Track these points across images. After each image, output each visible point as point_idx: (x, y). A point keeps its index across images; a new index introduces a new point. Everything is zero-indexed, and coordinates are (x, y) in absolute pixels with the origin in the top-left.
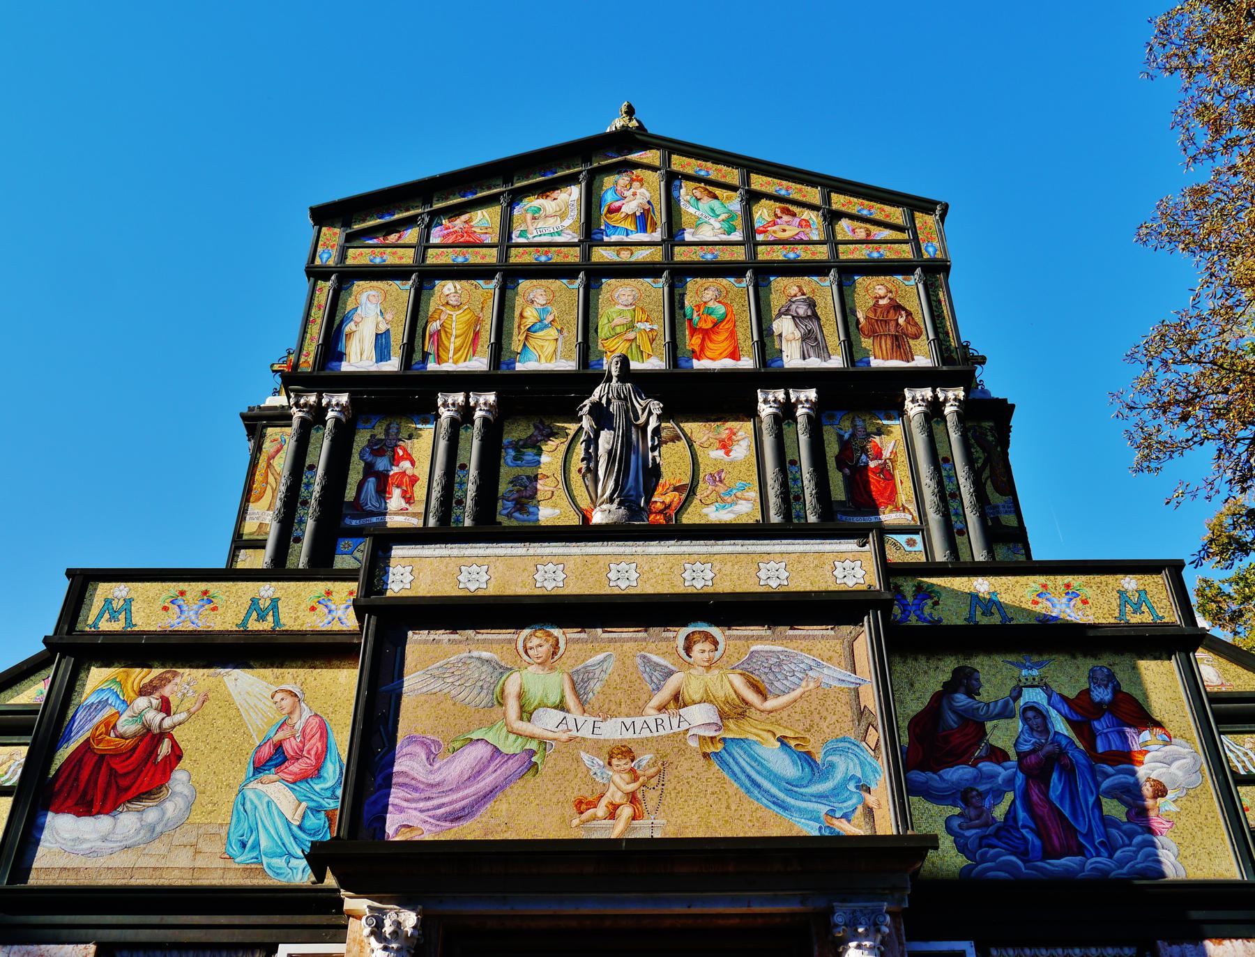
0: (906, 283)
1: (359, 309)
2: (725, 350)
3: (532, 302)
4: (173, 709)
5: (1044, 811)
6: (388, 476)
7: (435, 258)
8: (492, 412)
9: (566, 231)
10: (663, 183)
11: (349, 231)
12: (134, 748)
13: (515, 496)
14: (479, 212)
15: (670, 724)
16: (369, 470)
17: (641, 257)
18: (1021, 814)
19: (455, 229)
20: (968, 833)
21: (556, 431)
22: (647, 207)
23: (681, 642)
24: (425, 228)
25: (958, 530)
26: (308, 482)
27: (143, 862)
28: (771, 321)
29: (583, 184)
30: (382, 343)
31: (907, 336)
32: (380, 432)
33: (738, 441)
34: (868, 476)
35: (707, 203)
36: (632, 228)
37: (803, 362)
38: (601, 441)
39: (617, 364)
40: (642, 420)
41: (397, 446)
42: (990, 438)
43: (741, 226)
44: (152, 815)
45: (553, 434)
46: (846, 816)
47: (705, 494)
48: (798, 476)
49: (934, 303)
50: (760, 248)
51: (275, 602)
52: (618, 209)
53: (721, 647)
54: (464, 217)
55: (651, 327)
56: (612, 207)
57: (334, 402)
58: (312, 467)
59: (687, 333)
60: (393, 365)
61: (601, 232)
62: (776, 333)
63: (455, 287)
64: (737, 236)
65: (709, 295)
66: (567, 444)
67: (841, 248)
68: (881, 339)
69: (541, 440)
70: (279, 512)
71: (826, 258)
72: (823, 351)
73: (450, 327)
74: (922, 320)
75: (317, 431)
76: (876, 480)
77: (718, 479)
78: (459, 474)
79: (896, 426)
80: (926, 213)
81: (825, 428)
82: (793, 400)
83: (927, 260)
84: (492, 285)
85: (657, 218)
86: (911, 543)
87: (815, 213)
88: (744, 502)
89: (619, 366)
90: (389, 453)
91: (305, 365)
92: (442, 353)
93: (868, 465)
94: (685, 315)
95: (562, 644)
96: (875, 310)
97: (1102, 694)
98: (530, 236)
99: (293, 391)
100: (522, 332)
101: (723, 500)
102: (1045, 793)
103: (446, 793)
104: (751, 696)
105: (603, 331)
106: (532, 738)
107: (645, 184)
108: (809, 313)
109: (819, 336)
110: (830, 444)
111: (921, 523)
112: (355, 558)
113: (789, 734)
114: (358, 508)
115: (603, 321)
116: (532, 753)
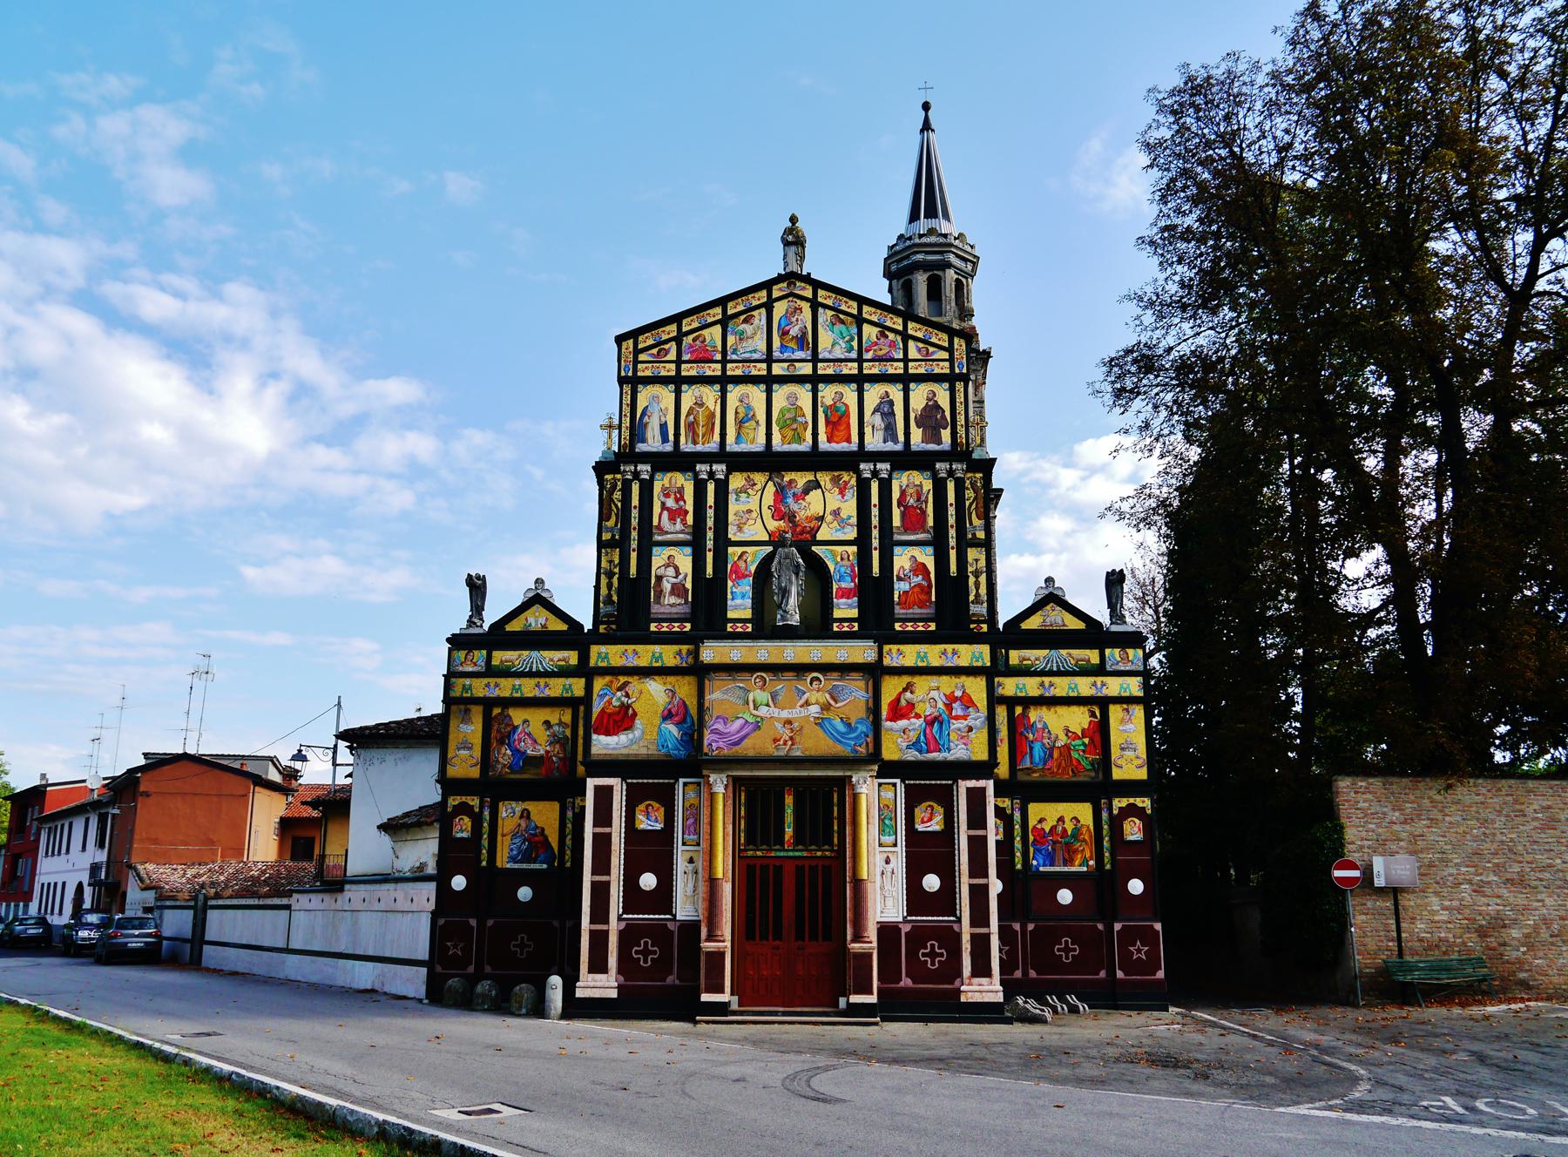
5: (929, 736)
7: (689, 370)
12: (620, 712)
15: (804, 712)
18: (922, 738)
23: (809, 681)
27: (631, 752)
36: (795, 347)
44: (631, 736)
51: (661, 654)
60: (669, 447)
72: (896, 441)
97: (958, 694)
114: (659, 527)
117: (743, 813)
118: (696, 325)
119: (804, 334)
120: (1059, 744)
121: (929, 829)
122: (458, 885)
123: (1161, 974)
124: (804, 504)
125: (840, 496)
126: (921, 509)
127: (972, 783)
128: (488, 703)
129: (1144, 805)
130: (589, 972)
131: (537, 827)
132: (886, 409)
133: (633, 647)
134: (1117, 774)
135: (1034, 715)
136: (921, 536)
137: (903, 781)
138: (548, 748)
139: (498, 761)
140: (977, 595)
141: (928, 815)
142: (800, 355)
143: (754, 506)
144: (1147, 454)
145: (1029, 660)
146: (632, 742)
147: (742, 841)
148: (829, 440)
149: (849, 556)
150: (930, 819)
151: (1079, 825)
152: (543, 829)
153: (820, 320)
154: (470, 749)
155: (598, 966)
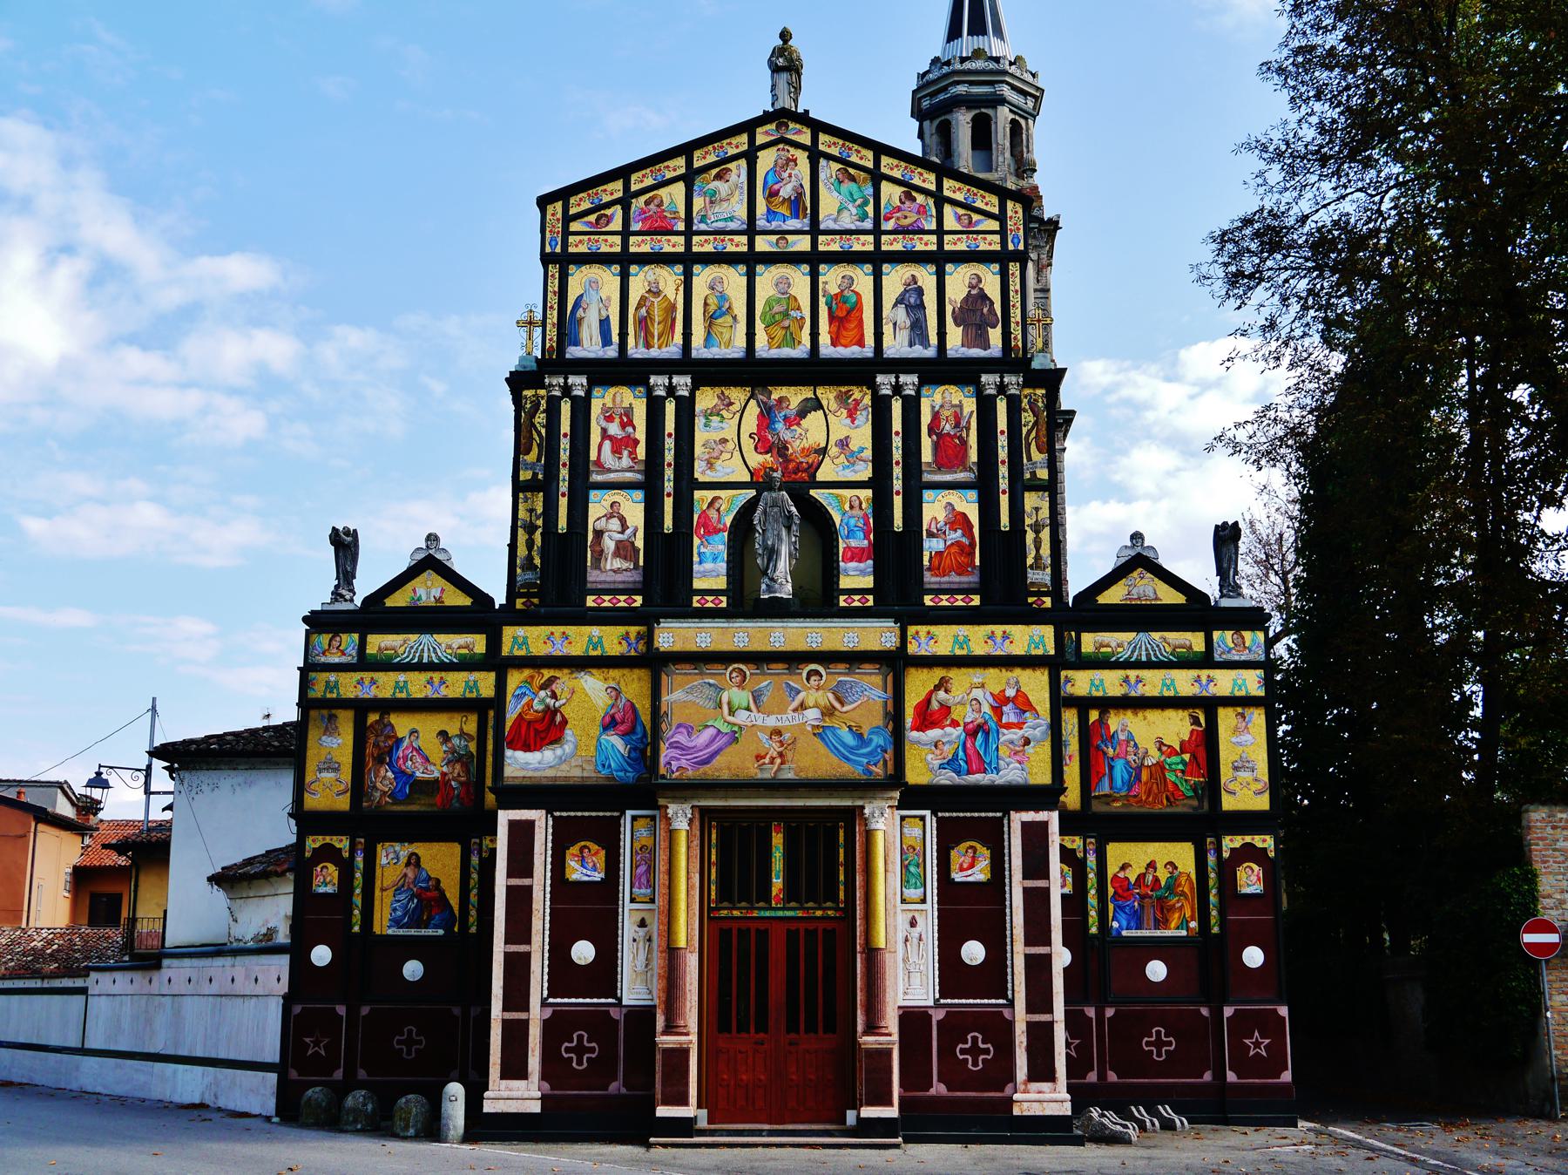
4: (558, 694)
5: (971, 752)
7: (639, 245)
12: (544, 718)
13: (707, 457)
15: (798, 719)
18: (961, 754)
20: (935, 762)
23: (804, 675)
36: (787, 214)
37: (909, 349)
42: (1040, 404)
44: (559, 752)
46: (875, 765)
51: (600, 638)
52: (776, 193)
53: (824, 678)
60: (612, 352)
67: (947, 238)
72: (925, 342)
81: (923, 400)
92: (649, 338)
95: (748, 673)
97: (1011, 693)
102: (974, 744)
103: (696, 752)
104: (837, 705)
106: (735, 725)
113: (853, 724)
114: (598, 463)
116: (736, 732)
117: (713, 858)
118: (649, 182)
119: (800, 196)
120: (1149, 762)
121: (970, 879)
122: (321, 958)
123: (1287, 1076)
124: (799, 431)
125: (849, 420)
126: (960, 438)
127: (1029, 816)
128: (360, 707)
129: (1265, 845)
130: (503, 1077)
131: (429, 878)
132: (912, 300)
133: (563, 628)
134: (1228, 803)
135: (1115, 721)
136: (961, 476)
137: (934, 813)
138: (445, 769)
139: (374, 787)
140: (1038, 557)
141: (968, 860)
142: (793, 224)
143: (730, 433)
144: (1272, 364)
145: (1108, 646)
146: (562, 760)
147: (713, 896)
148: (834, 343)
149: (861, 504)
150: (972, 866)
151: (1176, 873)
152: (438, 881)
153: (822, 176)
154: (336, 770)
155: (515, 1068)
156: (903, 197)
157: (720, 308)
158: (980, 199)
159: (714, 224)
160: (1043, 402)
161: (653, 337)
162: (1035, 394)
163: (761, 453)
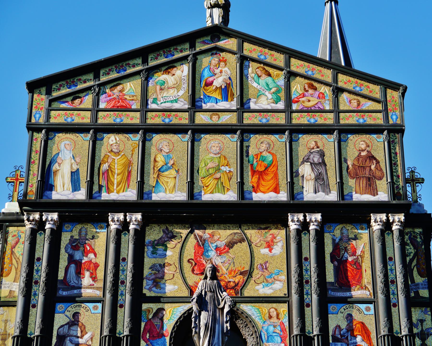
0: (378, 140)
1: (60, 154)
2: (271, 187)
3: (161, 150)
6: (81, 263)
8: (139, 225)
9: (180, 100)
10: (238, 64)
11: (51, 98)
13: (153, 277)
14: (128, 83)
16: (71, 259)
17: (224, 120)
19: (114, 96)
21: (175, 234)
22: (228, 81)
24: (96, 95)
25: (393, 304)
26: (38, 269)
28: (298, 166)
29: (191, 64)
30: (75, 178)
31: (375, 178)
32: (75, 234)
33: (277, 242)
34: (347, 266)
35: (265, 79)
36: (219, 97)
38: (202, 317)
39: (210, 271)
40: (221, 306)
41: (86, 243)
42: (419, 240)
43: (284, 98)
45: (173, 237)
47: (257, 277)
48: (308, 268)
49: (393, 155)
50: (294, 115)
52: (211, 84)
54: (119, 88)
55: (229, 169)
56: (208, 81)
57: (50, 219)
58: (39, 259)
59: (250, 173)
61: (201, 100)
62: (301, 175)
63: (116, 139)
64: (281, 106)
65: (264, 147)
66: (181, 243)
67: (342, 115)
68: (360, 179)
69: (167, 241)
70: (23, 290)
71: (332, 123)
72: (326, 189)
73: (114, 167)
74: (385, 166)
75: (41, 235)
76: (352, 269)
77: (264, 267)
78: (122, 264)
79: (364, 234)
80: (394, 90)
82: (308, 220)
83: (392, 125)
84: (138, 137)
85: (234, 91)
86: (368, 309)
87: (328, 87)
88: (278, 282)
89: (211, 272)
90: (81, 249)
91: (31, 193)
92: (110, 186)
93: (348, 260)
94: (249, 162)
96: (358, 159)
98: (159, 103)
99: (26, 211)
100: (155, 172)
101: (267, 281)
105: (202, 173)
107: (228, 64)
108: (320, 161)
109: (325, 178)
110: (328, 245)
111: (374, 298)
112: (66, 316)
114: (65, 281)
115: (202, 165)
142: (223, 105)
156: (307, 87)
157: (166, 164)
158: (365, 88)
159: (163, 105)
160: (421, 238)
161: (113, 184)
162: (414, 232)
163: (197, 274)
